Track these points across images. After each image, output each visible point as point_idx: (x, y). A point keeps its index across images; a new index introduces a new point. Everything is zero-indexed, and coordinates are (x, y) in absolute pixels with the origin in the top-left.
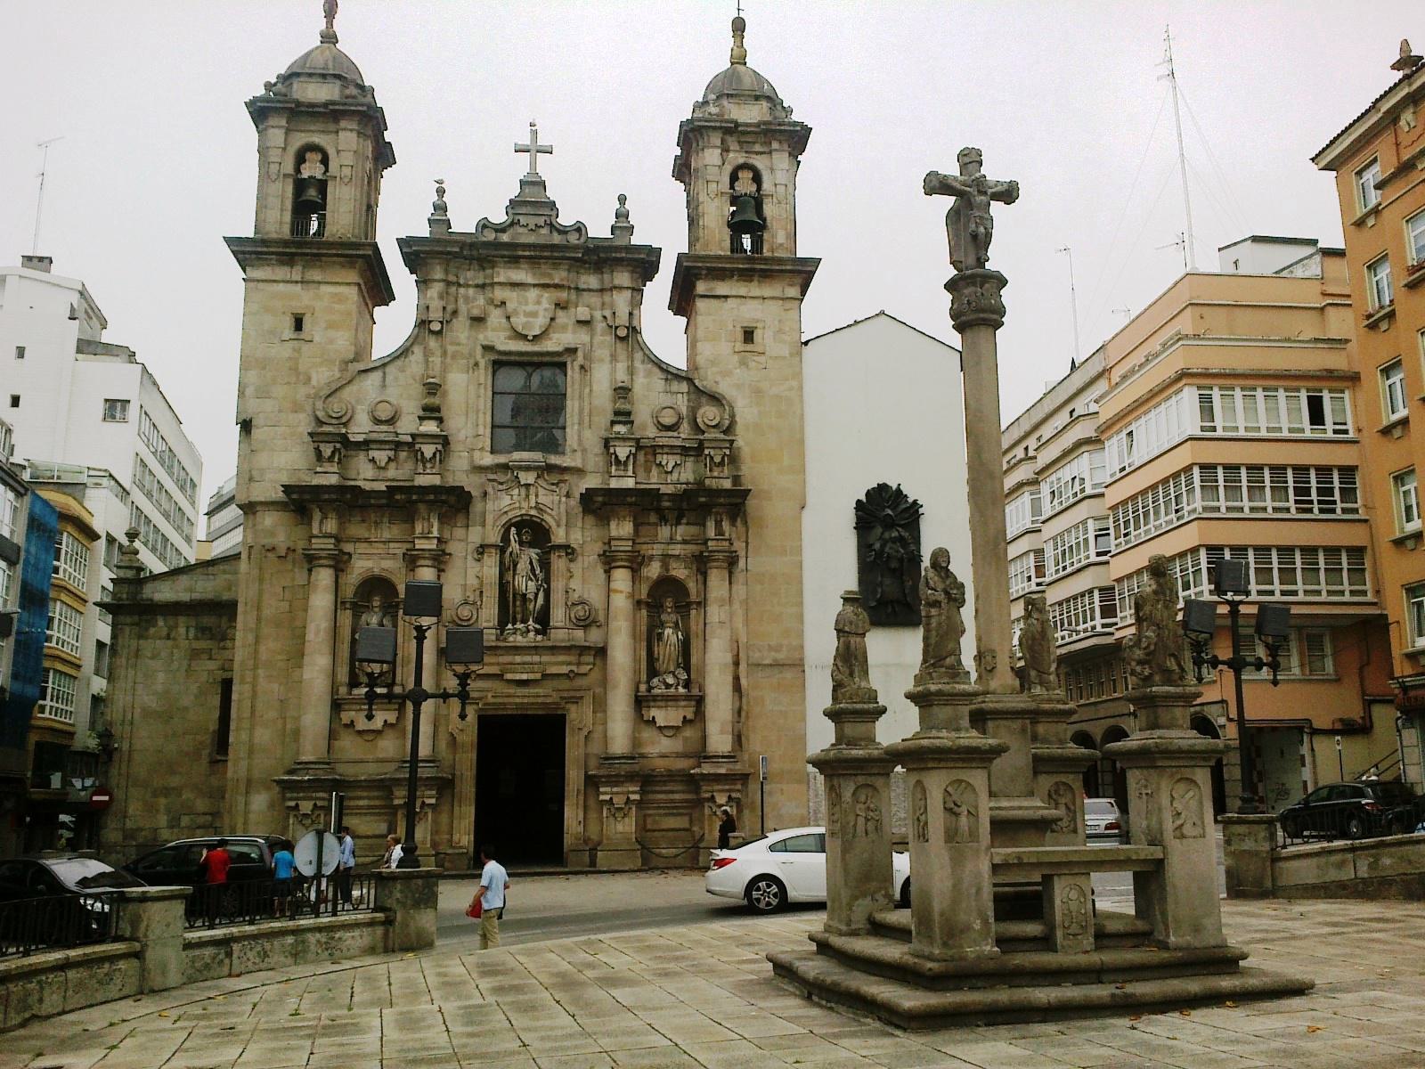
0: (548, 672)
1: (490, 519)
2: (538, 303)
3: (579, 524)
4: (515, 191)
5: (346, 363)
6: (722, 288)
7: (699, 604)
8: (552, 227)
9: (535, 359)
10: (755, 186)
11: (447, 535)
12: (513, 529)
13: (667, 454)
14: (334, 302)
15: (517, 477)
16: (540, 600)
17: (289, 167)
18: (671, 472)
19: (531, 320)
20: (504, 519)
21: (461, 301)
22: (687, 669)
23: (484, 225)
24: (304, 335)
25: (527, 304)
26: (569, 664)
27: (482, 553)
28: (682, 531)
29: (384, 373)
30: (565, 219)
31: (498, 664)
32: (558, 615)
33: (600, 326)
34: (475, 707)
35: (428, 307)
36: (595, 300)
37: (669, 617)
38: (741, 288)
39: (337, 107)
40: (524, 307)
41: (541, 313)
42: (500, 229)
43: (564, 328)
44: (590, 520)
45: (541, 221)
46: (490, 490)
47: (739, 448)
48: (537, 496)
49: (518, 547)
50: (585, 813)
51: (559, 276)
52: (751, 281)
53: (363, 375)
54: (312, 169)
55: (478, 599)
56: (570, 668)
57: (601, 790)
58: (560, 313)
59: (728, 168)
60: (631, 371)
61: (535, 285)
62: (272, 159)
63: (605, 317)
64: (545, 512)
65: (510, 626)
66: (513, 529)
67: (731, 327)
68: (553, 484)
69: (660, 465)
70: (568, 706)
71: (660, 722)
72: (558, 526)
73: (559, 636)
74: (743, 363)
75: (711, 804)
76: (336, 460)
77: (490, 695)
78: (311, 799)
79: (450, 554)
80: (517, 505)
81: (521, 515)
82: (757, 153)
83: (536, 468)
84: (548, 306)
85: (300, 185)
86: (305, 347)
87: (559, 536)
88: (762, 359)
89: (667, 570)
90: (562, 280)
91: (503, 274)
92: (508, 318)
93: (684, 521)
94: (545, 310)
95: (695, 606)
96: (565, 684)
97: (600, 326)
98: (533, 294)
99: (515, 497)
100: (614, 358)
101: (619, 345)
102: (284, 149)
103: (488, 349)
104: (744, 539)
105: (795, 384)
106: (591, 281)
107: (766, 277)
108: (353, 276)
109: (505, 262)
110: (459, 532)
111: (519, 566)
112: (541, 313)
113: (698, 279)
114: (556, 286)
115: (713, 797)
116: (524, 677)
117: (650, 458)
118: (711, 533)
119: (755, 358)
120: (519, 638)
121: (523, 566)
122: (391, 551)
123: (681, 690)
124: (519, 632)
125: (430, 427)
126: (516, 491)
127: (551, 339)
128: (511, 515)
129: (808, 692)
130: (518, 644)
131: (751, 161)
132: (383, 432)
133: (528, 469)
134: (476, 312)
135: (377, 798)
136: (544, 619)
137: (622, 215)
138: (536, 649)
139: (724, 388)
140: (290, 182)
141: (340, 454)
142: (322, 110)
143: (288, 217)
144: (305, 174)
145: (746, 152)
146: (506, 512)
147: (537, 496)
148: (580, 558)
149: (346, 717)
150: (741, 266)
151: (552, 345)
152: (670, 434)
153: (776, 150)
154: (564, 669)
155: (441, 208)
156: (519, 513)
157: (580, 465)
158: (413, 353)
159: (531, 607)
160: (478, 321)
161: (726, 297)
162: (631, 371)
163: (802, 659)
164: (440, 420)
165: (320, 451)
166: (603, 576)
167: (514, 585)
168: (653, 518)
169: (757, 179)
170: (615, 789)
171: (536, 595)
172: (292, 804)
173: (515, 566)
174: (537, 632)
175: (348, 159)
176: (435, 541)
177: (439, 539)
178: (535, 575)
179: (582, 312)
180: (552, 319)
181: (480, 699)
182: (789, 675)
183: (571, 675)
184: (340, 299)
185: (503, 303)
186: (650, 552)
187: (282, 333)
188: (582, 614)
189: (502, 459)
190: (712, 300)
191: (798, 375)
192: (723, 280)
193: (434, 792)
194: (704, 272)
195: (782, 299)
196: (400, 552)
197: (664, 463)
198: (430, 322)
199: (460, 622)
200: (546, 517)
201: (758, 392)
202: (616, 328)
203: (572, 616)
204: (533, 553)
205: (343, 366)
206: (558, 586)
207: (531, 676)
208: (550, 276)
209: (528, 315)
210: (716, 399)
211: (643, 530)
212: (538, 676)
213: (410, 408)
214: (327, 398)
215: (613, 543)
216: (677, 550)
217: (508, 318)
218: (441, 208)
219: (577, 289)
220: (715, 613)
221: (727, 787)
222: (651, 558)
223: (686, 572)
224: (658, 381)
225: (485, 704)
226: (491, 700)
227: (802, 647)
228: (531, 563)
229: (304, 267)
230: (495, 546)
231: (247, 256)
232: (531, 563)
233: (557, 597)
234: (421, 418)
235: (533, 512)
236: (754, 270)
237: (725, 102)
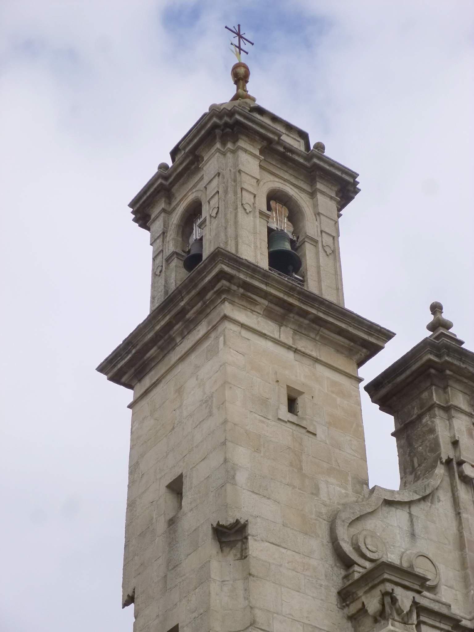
14: (333, 392)
39: (322, 164)
53: (386, 509)
62: (245, 186)
86: (307, 440)
142: (301, 161)
158: (439, 501)
187: (278, 409)
205: (358, 486)
229: (295, 332)
231: (234, 288)
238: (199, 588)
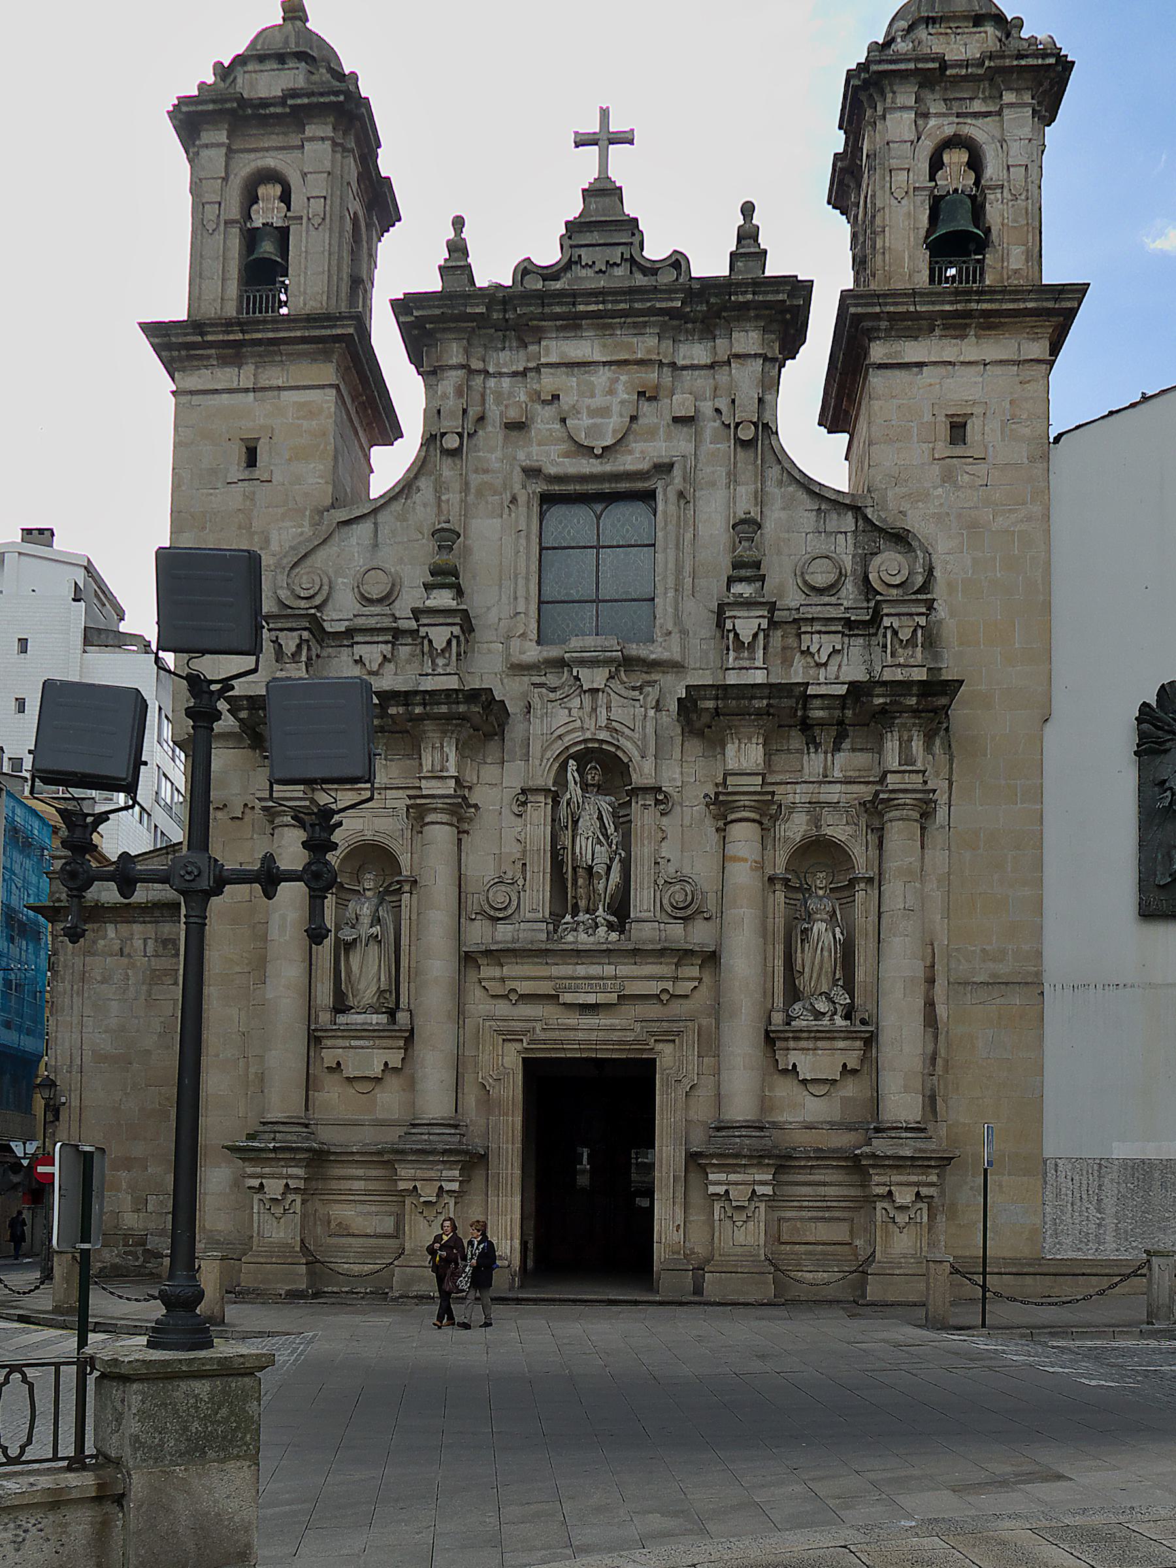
1: (535, 748)
2: (611, 392)
3: (677, 754)
4: (575, 208)
5: (321, 512)
6: (912, 351)
7: (870, 880)
8: (636, 263)
9: (606, 487)
10: (973, 175)
11: (470, 777)
12: (571, 762)
13: (819, 632)
15: (577, 678)
16: (615, 877)
17: (233, 211)
18: (825, 665)
19: (599, 421)
20: (558, 747)
21: (490, 399)
22: (849, 987)
23: (525, 269)
24: (259, 472)
25: (593, 396)
26: (661, 978)
27: (524, 804)
28: (844, 762)
29: (375, 524)
30: (655, 250)
31: (550, 978)
32: (642, 901)
33: (710, 426)
34: (518, 1046)
35: (439, 411)
36: (701, 382)
37: (820, 904)
38: (949, 349)
40: (588, 401)
41: (616, 409)
42: (550, 274)
43: (652, 433)
44: (695, 747)
45: (615, 255)
46: (536, 702)
47: (940, 622)
48: (609, 708)
49: (579, 791)
51: (646, 344)
52: (963, 337)
54: (268, 212)
55: (519, 875)
58: (646, 407)
59: (927, 146)
60: (760, 498)
61: (605, 363)
63: (718, 411)
65: (568, 918)
66: (571, 762)
67: (927, 417)
68: (634, 689)
69: (807, 653)
70: (659, 1046)
71: (805, 1073)
73: (643, 933)
74: (948, 477)
75: (885, 1205)
76: (304, 658)
77: (538, 1026)
78: (280, 1177)
79: (476, 806)
80: (578, 724)
81: (585, 741)
82: (976, 115)
83: (607, 662)
84: (626, 396)
85: (251, 238)
87: (643, 772)
88: (982, 468)
89: (818, 827)
90: (649, 352)
91: (556, 348)
92: (563, 420)
93: (846, 745)
94: (622, 402)
95: (862, 885)
96: (652, 1010)
97: (710, 426)
98: (602, 377)
99: (574, 712)
100: (733, 478)
101: (741, 454)
102: (225, 179)
103: (532, 473)
104: (945, 773)
105: (1036, 509)
106: (696, 352)
107: (990, 327)
108: (327, 372)
109: (559, 329)
110: (490, 772)
112: (616, 409)
113: (870, 340)
114: (641, 362)
115: (890, 1193)
116: (591, 999)
117: (792, 641)
118: (892, 760)
119: (968, 468)
120: (583, 937)
121: (588, 823)
122: (389, 804)
123: (839, 1022)
124: (582, 927)
125: (443, 599)
126: (576, 702)
127: (631, 452)
128: (568, 740)
129: (1048, 1029)
130: (581, 947)
131: (966, 130)
132: (374, 617)
133: (594, 663)
134: (513, 414)
135: (376, 1179)
136: (620, 909)
137: (748, 235)
138: (608, 953)
139: (916, 522)
140: (235, 231)
141: (309, 649)
143: (233, 289)
144: (258, 222)
145: (958, 115)
146: (560, 737)
147: (609, 708)
149: (329, 1057)
150: (947, 308)
151: (632, 460)
152: (826, 599)
153: (1011, 105)
154: (654, 988)
155: (458, 248)
156: (578, 736)
157: (677, 657)
159: (601, 887)
160: (517, 427)
161: (920, 365)
162: (760, 498)
163: (1039, 974)
164: (460, 593)
165: (280, 645)
166: (714, 837)
167: (573, 853)
168: (796, 740)
169: (975, 164)
171: (609, 868)
172: (255, 1183)
173: (575, 823)
174: (611, 927)
175: (318, 185)
176: (452, 783)
177: (457, 780)
178: (606, 836)
179: (682, 404)
180: (633, 418)
182: (1016, 999)
183: (665, 997)
184: (311, 413)
185: (556, 397)
186: (790, 798)
188: (679, 897)
189: (553, 652)
190: (897, 372)
191: (1042, 493)
192: (916, 338)
194: (884, 324)
195: (1018, 363)
196: (402, 804)
197: (813, 650)
198: (445, 433)
199: (492, 913)
200: (623, 742)
201: (973, 528)
202: (737, 425)
203: (665, 901)
204: (604, 803)
206: (642, 851)
207: (601, 999)
208: (630, 348)
209: (593, 413)
210: (901, 539)
211: (779, 760)
213: (414, 575)
214: (292, 568)
215: (730, 780)
216: (833, 793)
217: (563, 420)
218: (458, 248)
219: (673, 365)
220: (896, 893)
221: (914, 1178)
222: (792, 807)
223: (849, 829)
224: (805, 513)
227: (1039, 954)
228: (600, 818)
230: (547, 791)
232: (600, 818)
233: (642, 875)
234: (428, 587)
235: (603, 735)
236: (968, 314)
237: (922, 33)
238: (693, 359)
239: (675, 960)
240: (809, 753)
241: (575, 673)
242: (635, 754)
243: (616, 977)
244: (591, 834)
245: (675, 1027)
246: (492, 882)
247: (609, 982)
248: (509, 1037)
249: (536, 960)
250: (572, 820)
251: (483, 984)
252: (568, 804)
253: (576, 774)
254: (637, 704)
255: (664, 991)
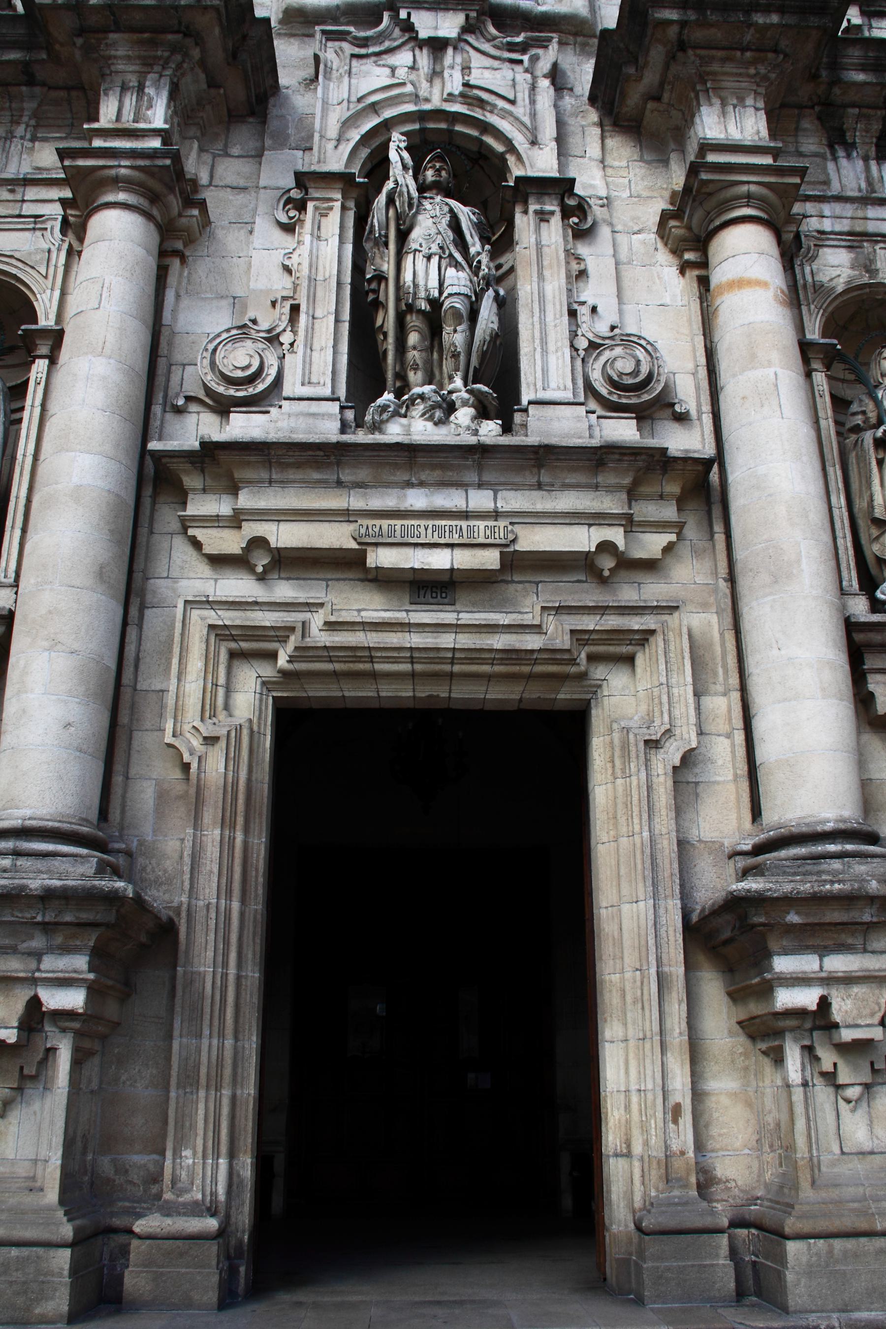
0: (523, 545)
34: (267, 671)
50: (696, 1076)
56: (599, 534)
57: (783, 964)
64: (493, 108)
65: (388, 397)
70: (599, 672)
72: (534, 143)
77: (317, 620)
80: (409, 88)
99: (402, 73)
111: (416, 234)
126: (404, 58)
148: (604, 232)
170: (838, 963)
173: (403, 236)
174: (483, 413)
181: (282, 633)
183: (607, 563)
193: (80, 963)
200: (493, 119)
203: (596, 377)
207: (464, 560)
212: (490, 559)
225: (302, 653)
226: (319, 637)
230: (344, 179)
239: (627, 481)
240: (835, 159)
241: (403, 14)
242: (519, 140)
243: (496, 515)
244: (435, 248)
245: (636, 623)
246: (225, 336)
247: (481, 524)
248: (244, 645)
249: (316, 476)
250: (398, 230)
251: (191, 532)
252: (390, 201)
253: (406, 155)
254: (519, 69)
255: (605, 547)
